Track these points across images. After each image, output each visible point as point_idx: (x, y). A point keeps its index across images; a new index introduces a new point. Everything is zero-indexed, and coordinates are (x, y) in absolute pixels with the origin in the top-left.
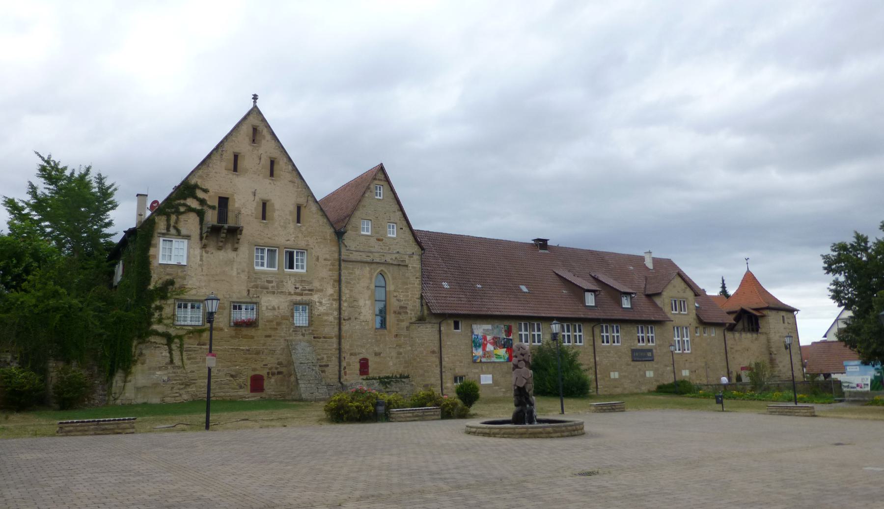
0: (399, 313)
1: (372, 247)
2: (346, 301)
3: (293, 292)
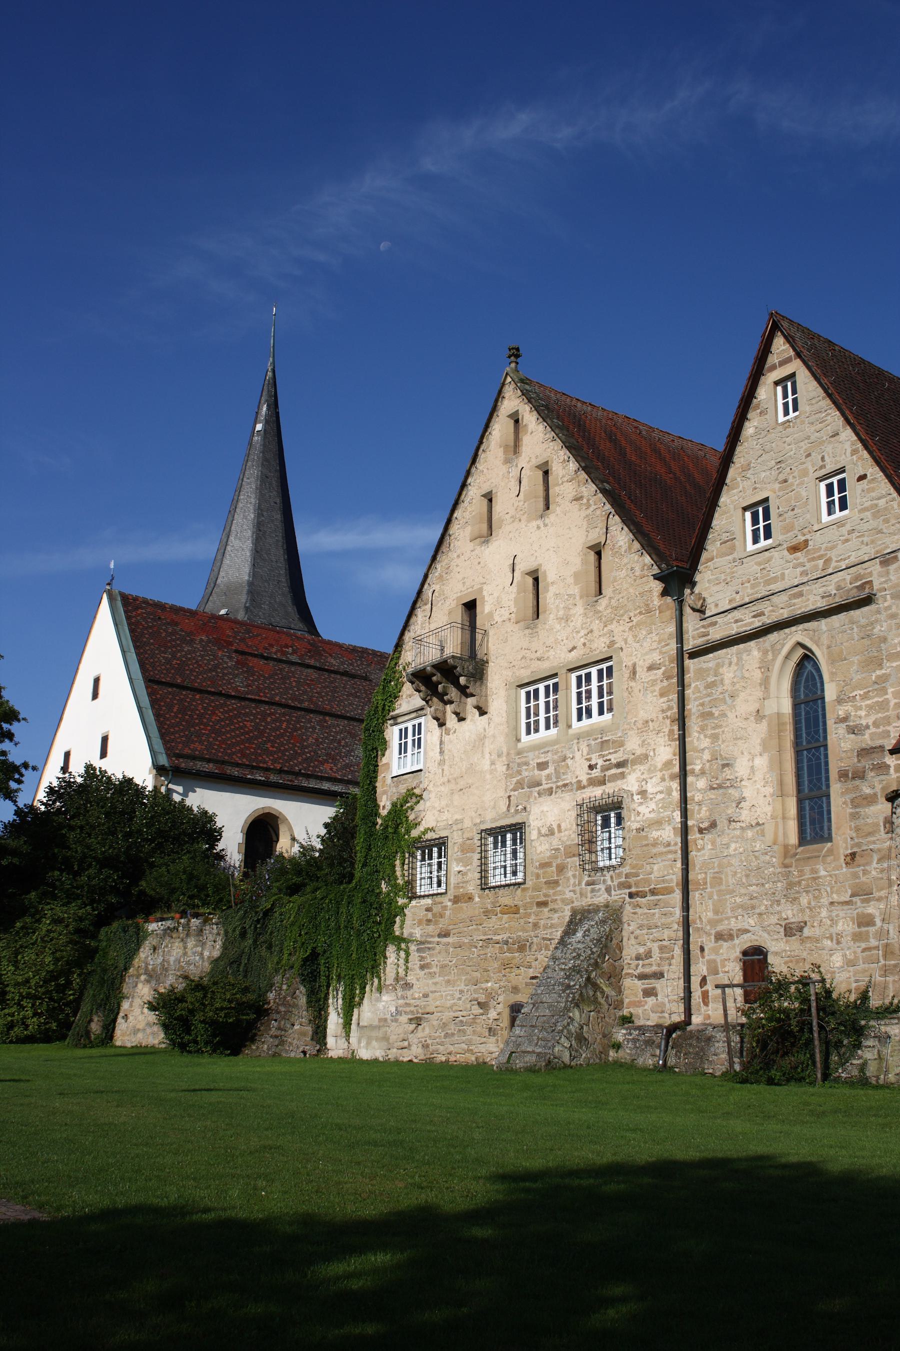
0: (860, 775)
1: (775, 580)
2: (703, 772)
3: (584, 778)
